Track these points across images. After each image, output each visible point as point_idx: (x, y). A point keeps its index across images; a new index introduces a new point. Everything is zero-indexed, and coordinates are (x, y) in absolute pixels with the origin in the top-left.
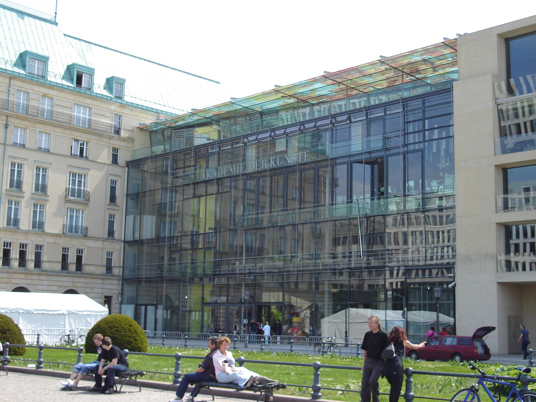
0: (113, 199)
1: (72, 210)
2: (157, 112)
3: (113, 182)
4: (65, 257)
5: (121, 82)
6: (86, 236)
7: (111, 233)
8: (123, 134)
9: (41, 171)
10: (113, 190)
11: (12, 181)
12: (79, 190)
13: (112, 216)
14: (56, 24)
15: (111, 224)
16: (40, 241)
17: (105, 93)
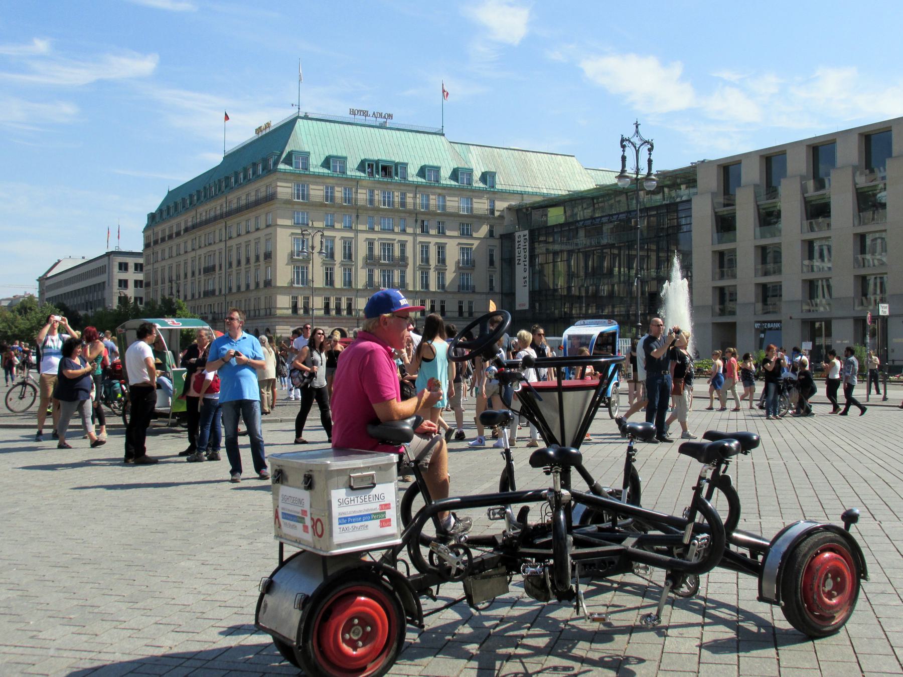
0: (492, 263)
1: (463, 274)
2: (521, 194)
3: (491, 251)
4: (461, 308)
5: (493, 175)
6: (474, 292)
7: (491, 288)
8: (497, 214)
9: (441, 248)
10: (491, 256)
11: (422, 258)
12: (467, 260)
13: (491, 276)
14: (443, 135)
15: (491, 281)
16: (443, 297)
17: (482, 185)
